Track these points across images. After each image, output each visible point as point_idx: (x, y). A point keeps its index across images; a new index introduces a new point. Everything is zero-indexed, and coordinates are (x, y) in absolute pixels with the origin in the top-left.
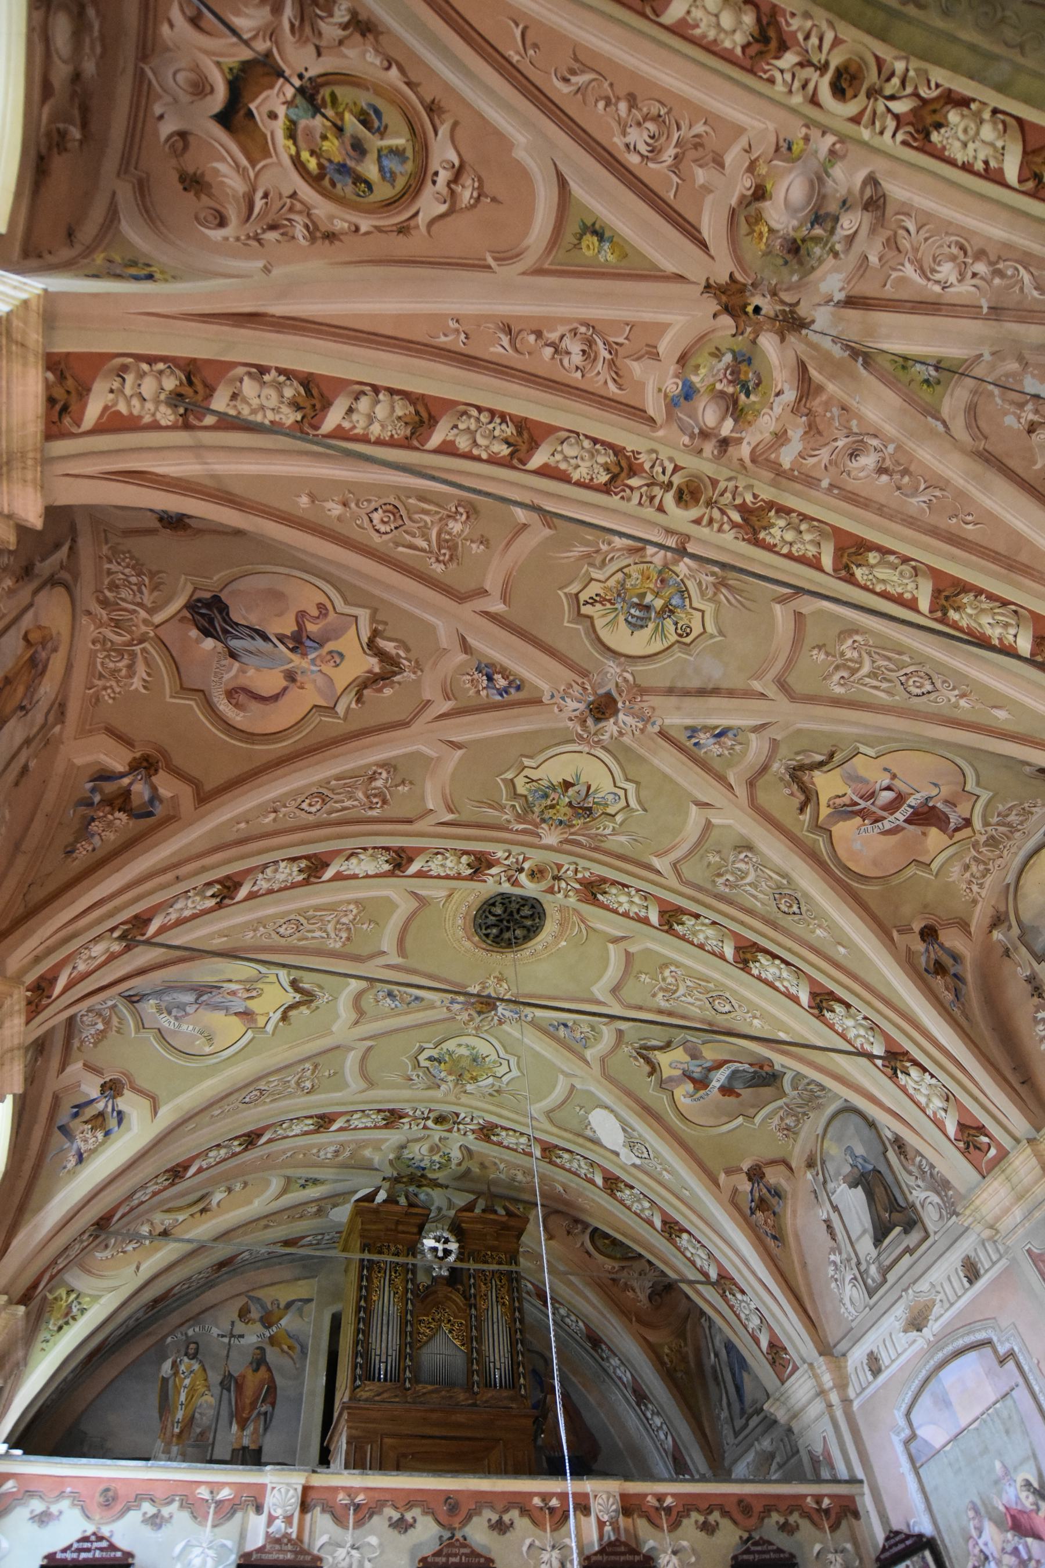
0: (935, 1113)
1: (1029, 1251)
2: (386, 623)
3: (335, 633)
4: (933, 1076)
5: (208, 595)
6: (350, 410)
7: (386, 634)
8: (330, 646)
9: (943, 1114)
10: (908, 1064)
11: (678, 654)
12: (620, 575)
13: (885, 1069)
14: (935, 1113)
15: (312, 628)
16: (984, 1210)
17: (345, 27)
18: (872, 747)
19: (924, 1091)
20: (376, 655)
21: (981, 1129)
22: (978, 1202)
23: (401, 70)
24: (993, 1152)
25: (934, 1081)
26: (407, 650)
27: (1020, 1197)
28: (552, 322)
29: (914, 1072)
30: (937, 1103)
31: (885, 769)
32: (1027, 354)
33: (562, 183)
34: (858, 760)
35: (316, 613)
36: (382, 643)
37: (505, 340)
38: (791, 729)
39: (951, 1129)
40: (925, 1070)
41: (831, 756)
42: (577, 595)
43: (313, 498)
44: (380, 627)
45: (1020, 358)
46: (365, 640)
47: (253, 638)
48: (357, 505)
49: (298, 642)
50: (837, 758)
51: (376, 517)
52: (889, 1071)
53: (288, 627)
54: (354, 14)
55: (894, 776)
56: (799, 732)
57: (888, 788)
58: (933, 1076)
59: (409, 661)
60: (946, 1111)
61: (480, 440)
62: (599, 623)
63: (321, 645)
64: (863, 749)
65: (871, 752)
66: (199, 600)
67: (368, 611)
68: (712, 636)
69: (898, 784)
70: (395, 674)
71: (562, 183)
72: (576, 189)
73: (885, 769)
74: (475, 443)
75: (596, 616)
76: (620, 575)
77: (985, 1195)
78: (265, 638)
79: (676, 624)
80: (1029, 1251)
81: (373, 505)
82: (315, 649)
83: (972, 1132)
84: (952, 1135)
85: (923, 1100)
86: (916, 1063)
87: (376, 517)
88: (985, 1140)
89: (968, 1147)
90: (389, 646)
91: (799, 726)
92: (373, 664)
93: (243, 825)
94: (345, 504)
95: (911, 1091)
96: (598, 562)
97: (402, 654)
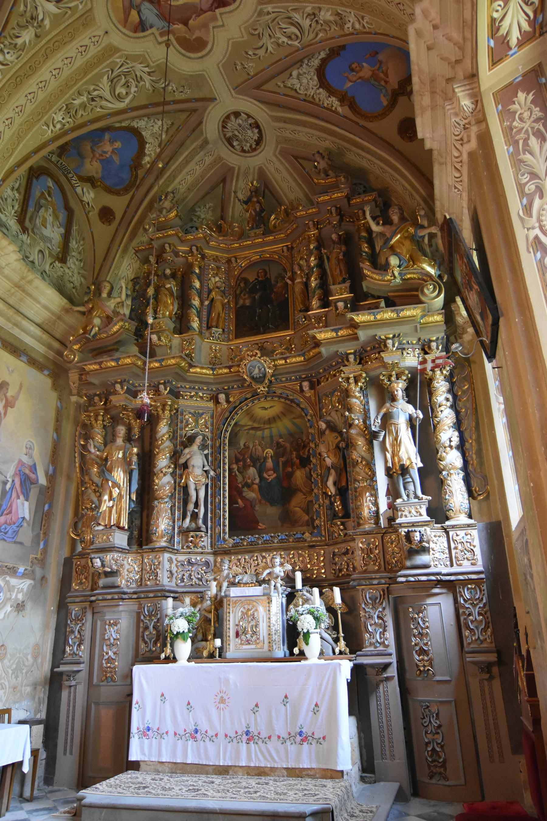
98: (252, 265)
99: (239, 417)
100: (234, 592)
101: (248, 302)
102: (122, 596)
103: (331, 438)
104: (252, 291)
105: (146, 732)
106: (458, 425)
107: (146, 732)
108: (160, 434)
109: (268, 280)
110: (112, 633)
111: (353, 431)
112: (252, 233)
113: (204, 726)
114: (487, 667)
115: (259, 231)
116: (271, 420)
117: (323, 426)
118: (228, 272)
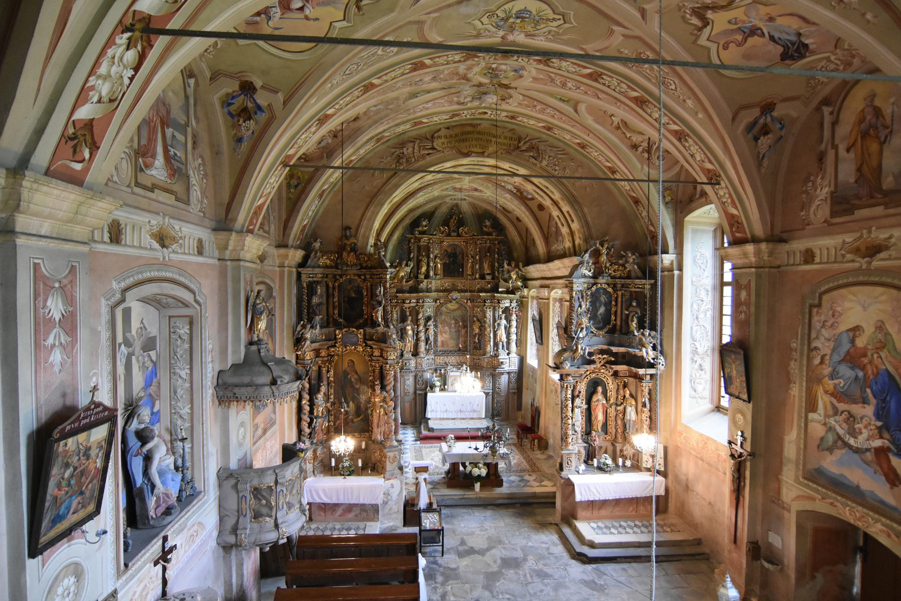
0: (92, 88)
1: (36, 266)
2: (692, 34)
3: (726, 33)
4: (132, 79)
5: (787, 62)
6: (668, 124)
7: (693, 27)
8: (735, 27)
9: (95, 99)
10: (139, 48)
11: (493, 7)
12: (538, 28)
13: (130, 14)
14: (92, 88)
15: (739, 37)
16: (38, 197)
17: (640, 146)
18: (340, 28)
19: (114, 69)
20: (706, 18)
21: (94, 147)
22: (45, 189)
23: (626, 137)
24: (78, 167)
25: (126, 81)
26: (683, 18)
27: (70, 221)
28: (579, 93)
29: (131, 56)
30: (105, 89)
31: (317, 19)
32: (389, 111)
33: (576, 111)
34: (340, 16)
35: (732, 45)
36: (699, 23)
37: (600, 96)
38: (398, 9)
39: (84, 113)
40: (136, 69)
41: (359, 8)
42: (565, 22)
43: (696, 113)
44: (696, 32)
45: (391, 109)
46: (709, 28)
47: (780, 38)
48: (679, 97)
49: (754, 31)
50: (354, 9)
51: (673, 87)
52: (129, 21)
53: (754, 41)
54: (637, 150)
55: (307, 18)
56: (392, 10)
57: (301, 9)
58: (132, 79)
59: (684, 11)
60: (99, 101)
61: (616, 84)
62: (549, 11)
63: (739, 28)
64: (344, 24)
65: (338, 25)
66: (794, 60)
67: (699, 42)
68: (474, 20)
69: (301, 16)
70: (698, 8)
71: (576, 111)
72: (572, 111)
73: (317, 19)
74: (618, 84)
75: (552, 14)
76: (538, 28)
77: (56, 192)
78: (772, 38)
79: (498, 17)
80: (36, 266)
81: (673, 92)
82: (744, 27)
83: (88, 138)
84: (74, 117)
85: (103, 70)
86: (142, 57)
87: (673, 87)
88: (87, 155)
89: (71, 139)
90: (695, 21)
91: (394, 14)
92: (710, 15)
93: (869, 16)
94: (685, 101)
95: (110, 52)
96: (553, 33)
97: (688, 16)
98: (450, 246)
99: (444, 309)
100: (452, 374)
101: (447, 262)
102: (412, 372)
103: (478, 324)
104: (449, 257)
105: (432, 411)
106: (516, 327)
107: (432, 411)
108: (419, 317)
109: (456, 253)
110: (408, 382)
111: (487, 325)
112: (453, 234)
113: (448, 409)
114: (514, 393)
115: (455, 234)
116: (454, 310)
117: (475, 319)
118: (442, 247)
